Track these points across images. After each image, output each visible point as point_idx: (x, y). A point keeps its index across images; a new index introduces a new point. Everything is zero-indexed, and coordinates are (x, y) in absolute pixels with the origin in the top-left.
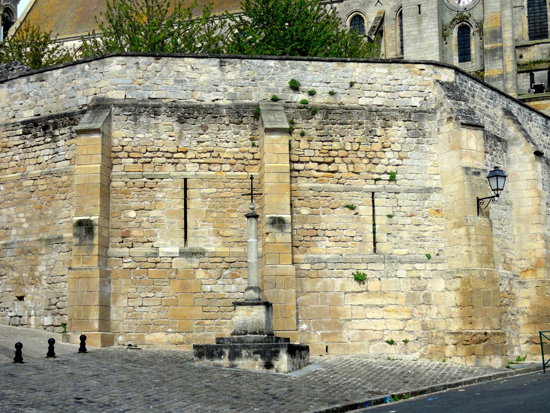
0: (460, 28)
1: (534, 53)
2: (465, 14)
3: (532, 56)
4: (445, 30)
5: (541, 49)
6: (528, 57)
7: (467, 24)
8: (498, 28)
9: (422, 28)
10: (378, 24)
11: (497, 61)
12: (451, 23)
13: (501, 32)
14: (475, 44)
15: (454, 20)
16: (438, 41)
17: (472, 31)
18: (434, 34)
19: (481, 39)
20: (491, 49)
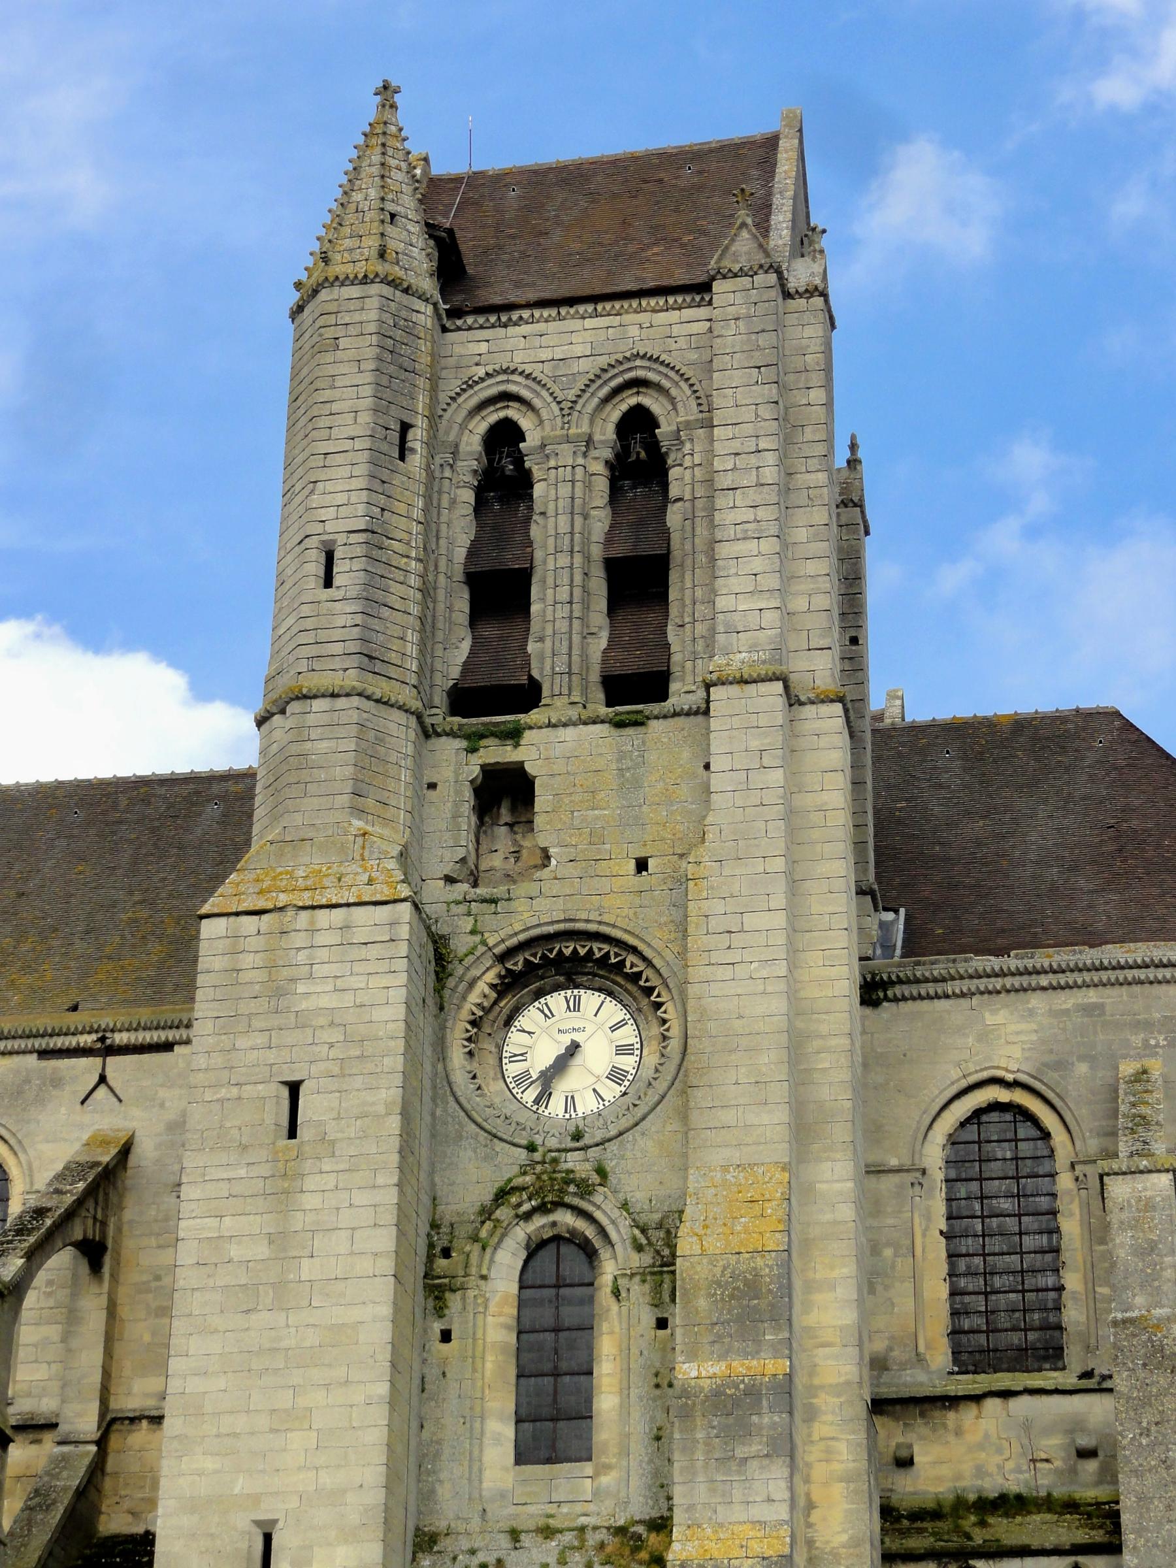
0: (535, 1249)
1: (981, 1447)
2: (577, 1164)
3: (967, 1468)
4: (446, 1253)
5: (1027, 1426)
6: (945, 1471)
7: (581, 1224)
8: (770, 1259)
9: (298, 1221)
10: (69, 1199)
11: (754, 1464)
12: (486, 1213)
13: (787, 1289)
14: (625, 1352)
15: (502, 1195)
16: (386, 1310)
17: (609, 1269)
18: (365, 1265)
19: (662, 1324)
20: (717, 1393)
